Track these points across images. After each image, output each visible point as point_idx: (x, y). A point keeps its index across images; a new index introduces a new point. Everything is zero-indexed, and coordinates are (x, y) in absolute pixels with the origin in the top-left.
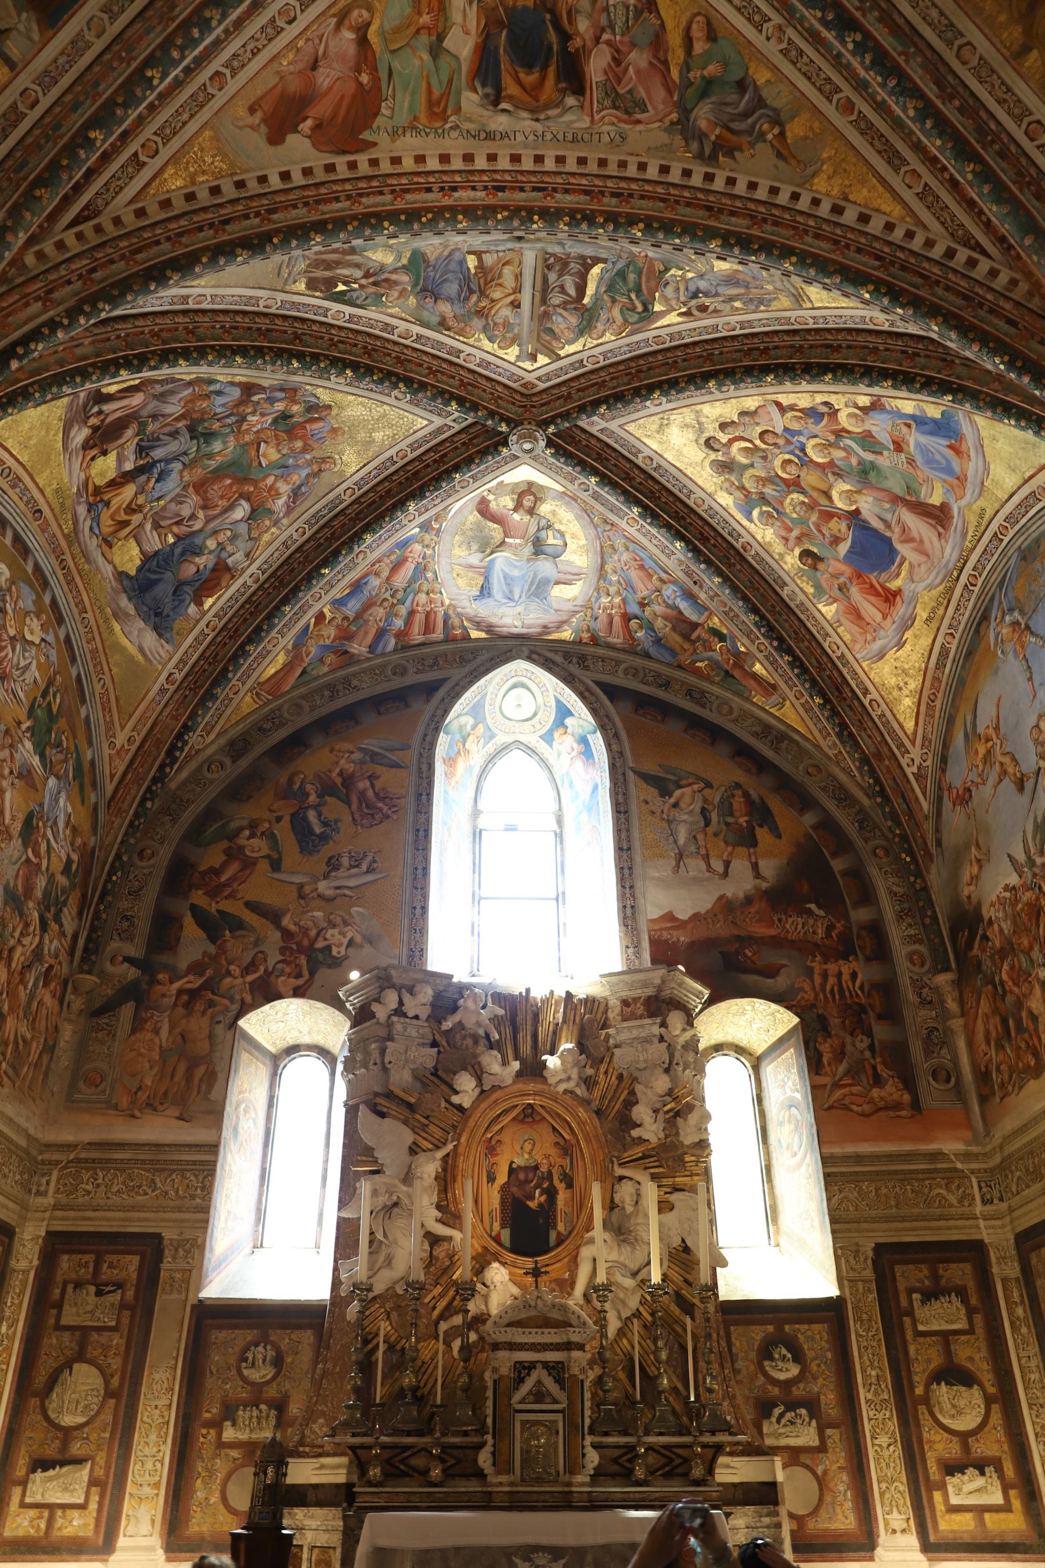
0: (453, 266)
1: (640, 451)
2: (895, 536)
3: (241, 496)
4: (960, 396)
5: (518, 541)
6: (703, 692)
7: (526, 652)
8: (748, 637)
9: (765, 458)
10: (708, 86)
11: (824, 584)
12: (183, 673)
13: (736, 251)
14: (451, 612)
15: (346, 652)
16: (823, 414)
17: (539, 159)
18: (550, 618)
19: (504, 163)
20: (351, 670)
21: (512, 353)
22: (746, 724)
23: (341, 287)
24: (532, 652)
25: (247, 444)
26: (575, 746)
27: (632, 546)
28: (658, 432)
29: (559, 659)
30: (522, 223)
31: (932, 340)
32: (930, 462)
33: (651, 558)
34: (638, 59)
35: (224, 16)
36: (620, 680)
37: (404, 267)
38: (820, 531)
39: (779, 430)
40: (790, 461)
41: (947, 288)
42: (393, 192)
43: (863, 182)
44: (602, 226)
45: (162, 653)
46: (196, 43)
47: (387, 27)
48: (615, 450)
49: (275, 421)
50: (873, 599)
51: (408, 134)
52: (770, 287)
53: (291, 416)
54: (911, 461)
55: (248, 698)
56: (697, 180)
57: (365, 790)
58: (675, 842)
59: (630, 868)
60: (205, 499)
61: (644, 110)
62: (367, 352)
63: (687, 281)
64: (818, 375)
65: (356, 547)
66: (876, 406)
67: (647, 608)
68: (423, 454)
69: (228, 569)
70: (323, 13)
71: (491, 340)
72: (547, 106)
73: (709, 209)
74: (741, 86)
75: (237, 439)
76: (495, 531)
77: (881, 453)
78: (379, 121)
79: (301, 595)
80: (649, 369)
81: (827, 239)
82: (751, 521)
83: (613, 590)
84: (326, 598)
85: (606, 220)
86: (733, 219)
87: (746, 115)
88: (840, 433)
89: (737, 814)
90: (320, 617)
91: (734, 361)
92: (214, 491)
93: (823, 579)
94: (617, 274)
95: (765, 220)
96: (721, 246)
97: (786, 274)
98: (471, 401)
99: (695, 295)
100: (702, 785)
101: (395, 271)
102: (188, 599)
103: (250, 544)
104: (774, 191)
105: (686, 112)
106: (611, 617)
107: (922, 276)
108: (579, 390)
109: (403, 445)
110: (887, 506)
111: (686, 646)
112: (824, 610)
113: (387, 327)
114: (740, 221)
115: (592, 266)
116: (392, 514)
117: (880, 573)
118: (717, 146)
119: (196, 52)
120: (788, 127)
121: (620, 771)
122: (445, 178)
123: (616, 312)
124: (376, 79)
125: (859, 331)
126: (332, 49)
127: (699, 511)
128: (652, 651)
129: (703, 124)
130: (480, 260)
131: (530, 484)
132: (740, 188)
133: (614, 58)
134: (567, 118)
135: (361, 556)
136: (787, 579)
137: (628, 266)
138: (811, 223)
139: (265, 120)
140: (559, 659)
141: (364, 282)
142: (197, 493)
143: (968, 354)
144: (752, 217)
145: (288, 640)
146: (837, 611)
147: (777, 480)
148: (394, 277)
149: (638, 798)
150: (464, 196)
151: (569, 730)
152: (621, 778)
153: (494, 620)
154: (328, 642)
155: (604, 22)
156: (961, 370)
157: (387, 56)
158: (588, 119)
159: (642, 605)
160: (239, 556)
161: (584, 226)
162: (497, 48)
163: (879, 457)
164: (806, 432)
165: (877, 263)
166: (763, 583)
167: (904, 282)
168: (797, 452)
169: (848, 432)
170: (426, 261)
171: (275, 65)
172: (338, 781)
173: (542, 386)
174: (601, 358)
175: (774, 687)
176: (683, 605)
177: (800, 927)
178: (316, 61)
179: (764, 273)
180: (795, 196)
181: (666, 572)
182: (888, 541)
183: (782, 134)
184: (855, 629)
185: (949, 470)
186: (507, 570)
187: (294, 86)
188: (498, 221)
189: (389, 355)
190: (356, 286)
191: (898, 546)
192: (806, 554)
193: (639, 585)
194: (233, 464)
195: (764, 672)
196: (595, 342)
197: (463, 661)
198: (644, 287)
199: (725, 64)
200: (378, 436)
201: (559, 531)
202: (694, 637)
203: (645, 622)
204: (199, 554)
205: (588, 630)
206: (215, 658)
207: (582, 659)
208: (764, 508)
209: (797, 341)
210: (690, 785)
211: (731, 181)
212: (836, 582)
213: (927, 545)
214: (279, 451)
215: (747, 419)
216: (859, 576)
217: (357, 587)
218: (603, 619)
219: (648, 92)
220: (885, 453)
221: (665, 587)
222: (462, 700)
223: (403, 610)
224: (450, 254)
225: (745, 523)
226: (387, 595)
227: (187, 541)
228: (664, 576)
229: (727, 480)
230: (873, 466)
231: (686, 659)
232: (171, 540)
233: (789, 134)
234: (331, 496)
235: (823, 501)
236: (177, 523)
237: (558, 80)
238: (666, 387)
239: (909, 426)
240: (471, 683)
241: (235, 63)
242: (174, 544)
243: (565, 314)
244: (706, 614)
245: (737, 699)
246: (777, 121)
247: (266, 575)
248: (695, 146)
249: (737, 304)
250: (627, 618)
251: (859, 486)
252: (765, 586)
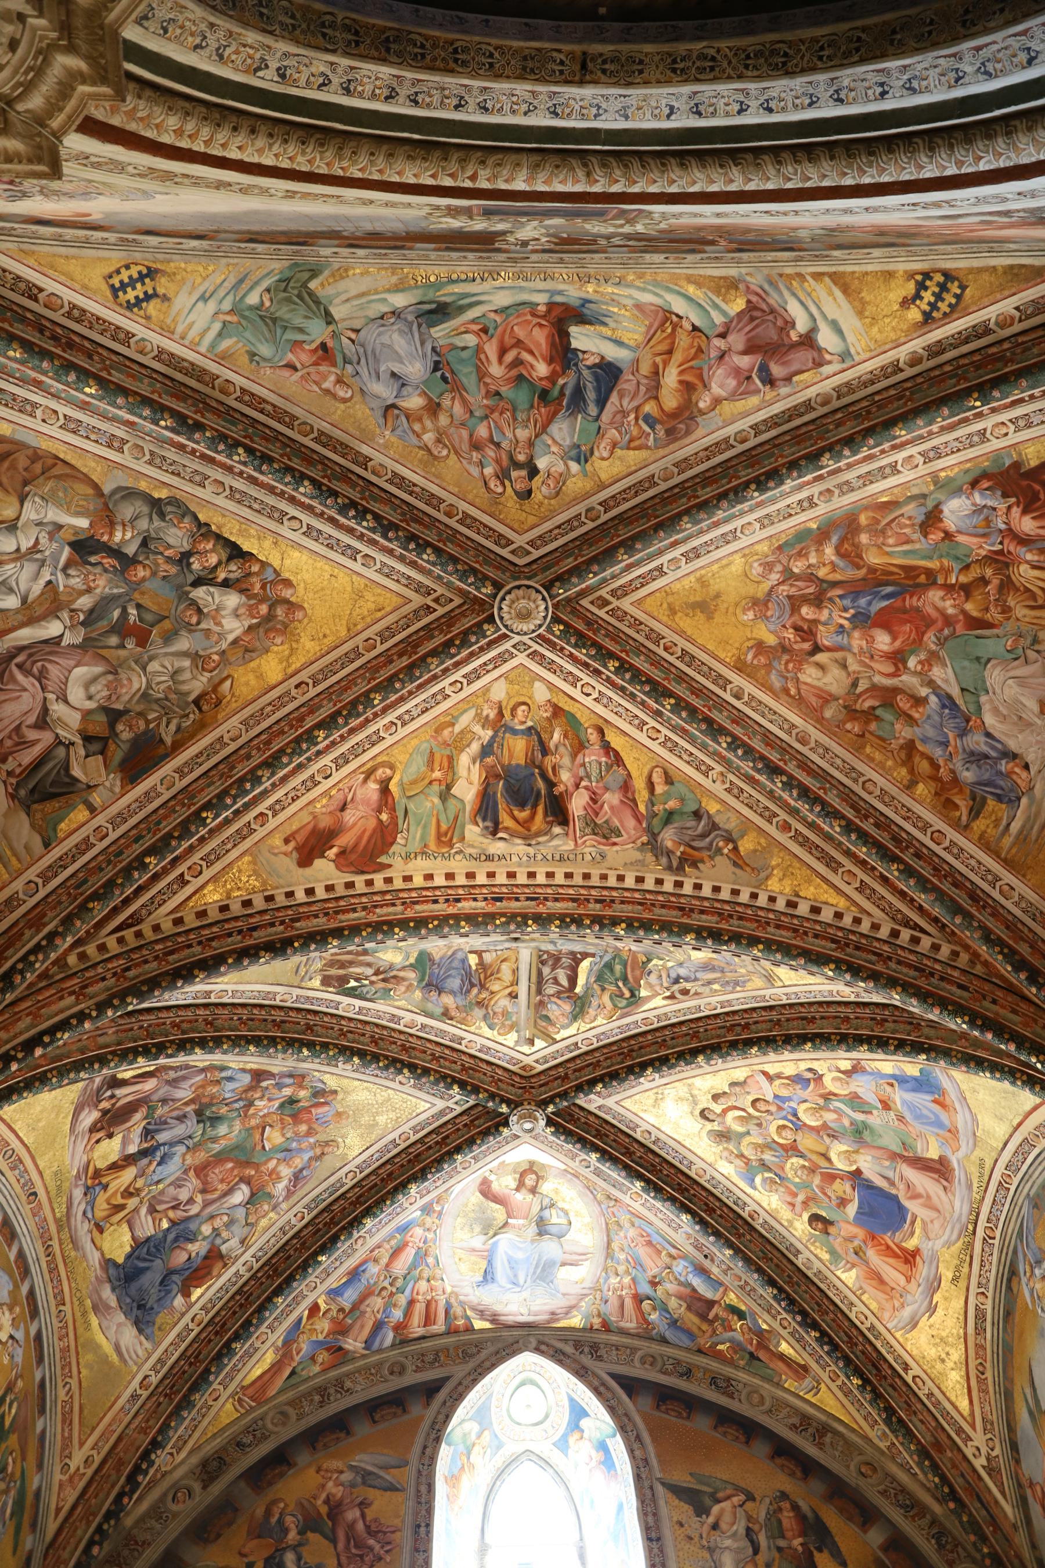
0: (456, 964)
1: (637, 1126)
2: (902, 1195)
3: (242, 1180)
4: (933, 1055)
5: (521, 1222)
6: (728, 1380)
7: (534, 1343)
8: (768, 1312)
9: (760, 1125)
10: (669, 817)
11: (839, 1249)
12: (160, 1376)
13: (709, 942)
14: (453, 1301)
15: (340, 1349)
16: (809, 1080)
17: (532, 875)
18: (557, 1303)
19: (501, 879)
20: (345, 1369)
21: (511, 1038)
22: (781, 1415)
23: (353, 983)
24: (541, 1343)
25: (252, 1128)
26: (593, 1453)
27: (637, 1221)
29: (569, 1349)
30: (518, 926)
31: (896, 1007)
32: (919, 1117)
33: (658, 1233)
34: (612, 798)
35: (273, 774)
36: (637, 1371)
37: (411, 965)
38: (825, 1194)
39: (770, 1097)
40: (784, 1127)
41: (899, 963)
42: (403, 904)
43: (809, 882)
44: (589, 927)
45: (140, 1352)
46: (247, 792)
47: (405, 780)
48: (614, 1126)
49: (282, 1106)
50: (891, 1261)
51: (419, 858)
52: (743, 971)
53: (298, 1101)
54: (901, 1118)
55: (229, 1406)
56: (668, 887)
57: (355, 1521)
60: (205, 1183)
61: (619, 835)
62: (374, 1041)
63: (668, 970)
64: (798, 1044)
65: (355, 1232)
66: (856, 1069)
67: (659, 1287)
68: (425, 1136)
69: (221, 1256)
70: (354, 771)
71: (491, 1027)
72: (538, 834)
73: (681, 909)
74: (697, 815)
75: (243, 1123)
76: (498, 1212)
77: (871, 1113)
78: (395, 848)
79: (295, 1284)
80: (641, 1048)
81: (787, 929)
82: (755, 1188)
83: (621, 1269)
84: (322, 1288)
85: (593, 922)
86: (704, 917)
87: (703, 836)
88: (828, 1096)
90: (314, 1309)
91: (719, 1037)
92: (215, 1174)
93: (837, 1243)
94: (605, 966)
95: (731, 916)
96: (696, 939)
97: (756, 959)
98: (472, 1084)
99: (676, 981)
100: (743, 1497)
101: (403, 969)
102: (175, 1289)
103: (247, 1229)
104: (735, 892)
105: (654, 836)
106: (621, 1299)
107: (875, 954)
108: (575, 1071)
109: (406, 1128)
110: (887, 1163)
111: (705, 1327)
112: (843, 1276)
113: (394, 1018)
114: (709, 918)
115: (582, 960)
116: (393, 1197)
117: (894, 1233)
118: (683, 860)
119: (246, 799)
120: (740, 843)
121: (647, 1484)
122: (450, 892)
123: (606, 998)
124: (394, 818)
125: (829, 1004)
126: (359, 796)
128: (668, 1335)
129: (669, 844)
130: (480, 957)
131: (532, 1163)
132: (706, 891)
133: (591, 799)
134: (555, 842)
135: (360, 1242)
136: (800, 1247)
137: (614, 959)
138: (771, 916)
139: (296, 849)
140: (569, 1349)
141: (374, 978)
142: (198, 1176)
143: (931, 1017)
144: (720, 914)
145: (278, 1336)
146: (857, 1277)
147: (774, 1146)
148: (402, 974)
150: (466, 906)
151: (586, 1435)
152: (648, 1492)
153: (498, 1308)
154: (321, 1337)
155: (582, 772)
156: (926, 1031)
157: (404, 800)
158: (572, 844)
159: (654, 1284)
160: (234, 1243)
161: (573, 928)
162: (495, 793)
164: (795, 1097)
165: (834, 946)
166: (776, 1253)
167: (860, 959)
168: (790, 1117)
169: (835, 1095)
170: (431, 960)
171: (310, 808)
172: (324, 1510)
173: (540, 1068)
175: (805, 1368)
176: (697, 1282)
178: (345, 804)
179: (736, 959)
180: (754, 896)
181: (674, 1247)
182: (895, 1199)
183: (736, 849)
184: (881, 1296)
185: (939, 1124)
186: (510, 1253)
187: (325, 822)
188: (497, 926)
189: (395, 1043)
190: (366, 982)
191: (906, 1203)
192: (815, 1218)
193: (647, 1262)
194: (237, 1147)
195: (791, 1351)
196: (588, 1026)
197: (467, 1356)
198: (629, 976)
199: (682, 800)
200: (382, 1119)
201: (562, 1210)
202: (711, 1316)
203: (658, 1302)
204: (191, 1241)
205: (599, 1315)
206: (197, 1357)
207: (595, 1348)
209: (774, 1015)
210: (728, 1498)
211: (698, 887)
212: (851, 1246)
213: (935, 1199)
214: (283, 1135)
215: (738, 1089)
216: (873, 1238)
217: (354, 1275)
218: (614, 1302)
219: (621, 822)
220: (875, 1112)
221: (675, 1263)
222: (465, 1403)
223: (402, 1300)
224: (454, 954)
225: (749, 1190)
226: (386, 1284)
227: (181, 1227)
228: (673, 1251)
229: (726, 1149)
230: (866, 1126)
231: (705, 1342)
232: (165, 1225)
233: (741, 849)
234: (332, 1180)
235: (823, 1163)
236: (173, 1208)
237: (546, 815)
238: (657, 1064)
239: (892, 1085)
240: (475, 1382)
241: (277, 807)
242: (168, 1229)
243: (559, 1002)
244: (721, 1289)
245: (767, 1386)
246: (729, 839)
247: (260, 1263)
248: (664, 860)
249: (716, 987)
250: (639, 1299)
251: (855, 1147)
252: (779, 1255)
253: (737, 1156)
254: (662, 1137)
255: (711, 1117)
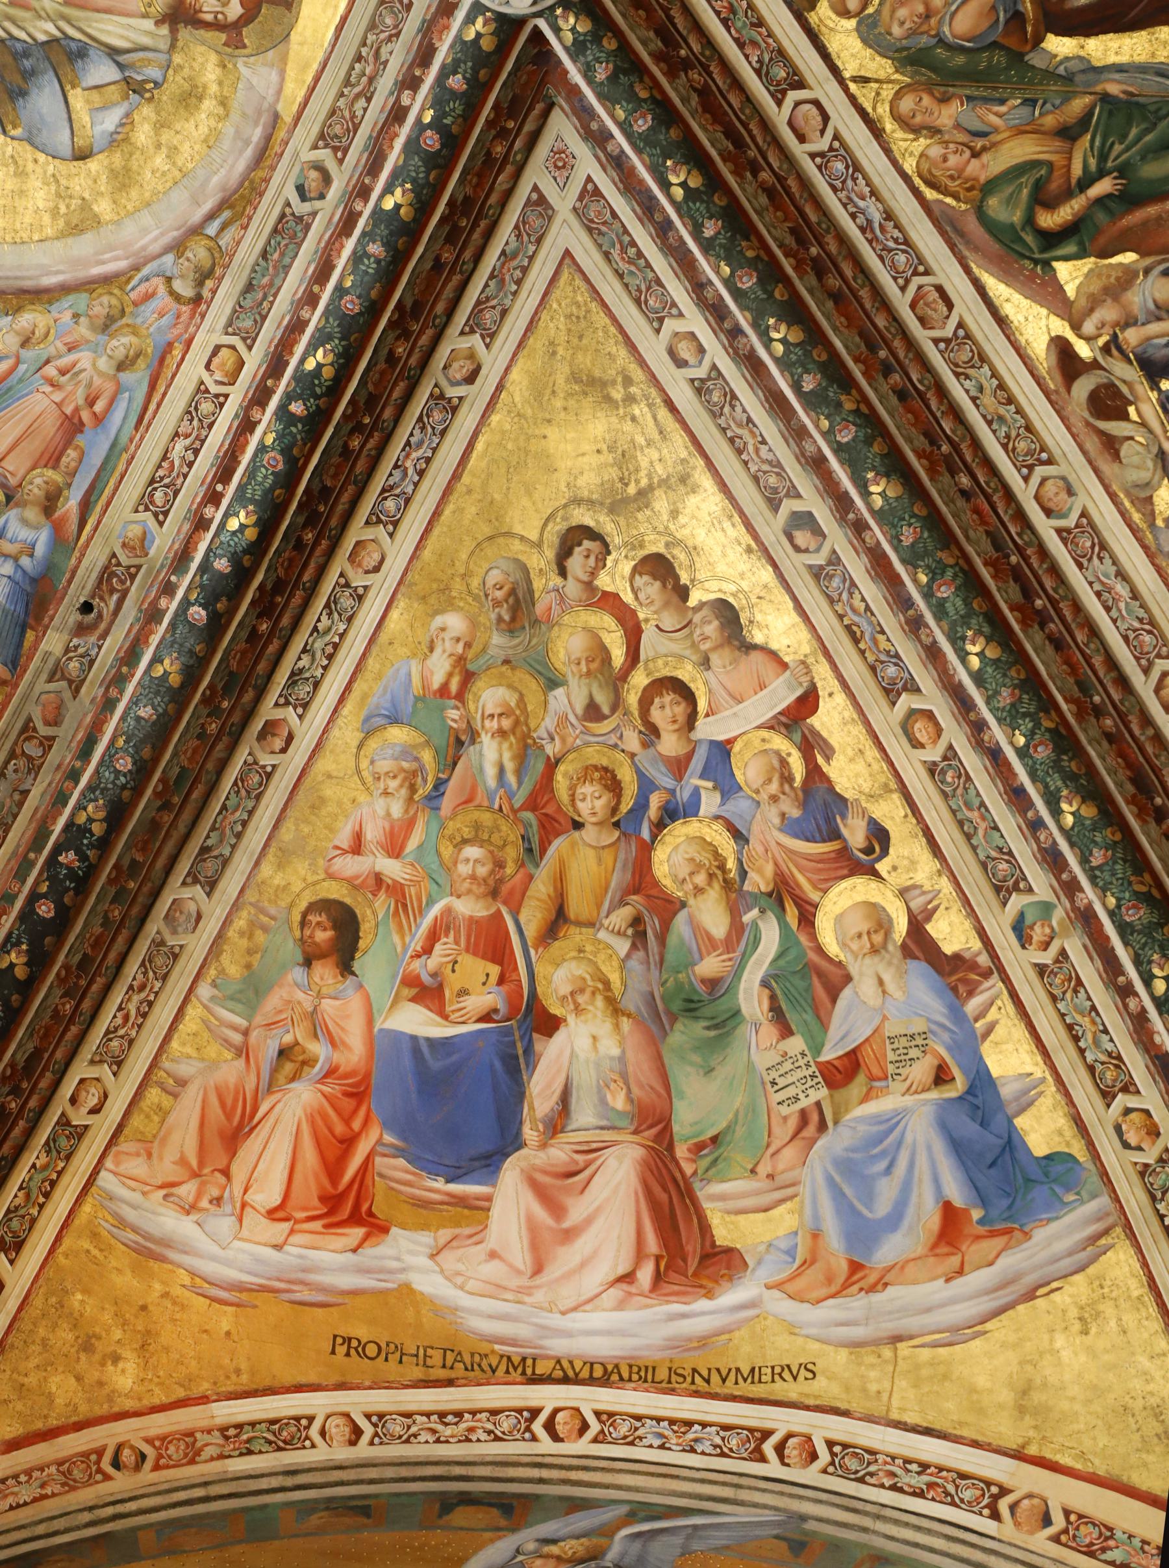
9: (593, 712)
16: (834, 835)
28: (575, 378)
40: (614, 786)
77: (786, 1032)
127: (339, 564)
147: (540, 766)
163: (769, 1032)
169: (807, 919)
174: (823, 144)
181: (86, 506)
196: (883, 110)
208: (427, 757)
215: (712, 629)
220: (796, 1044)
229: (474, 624)
235: (532, 917)
238: (820, 355)
251: (633, 1001)
253: (460, 660)
254: (466, 420)
255: (577, 563)
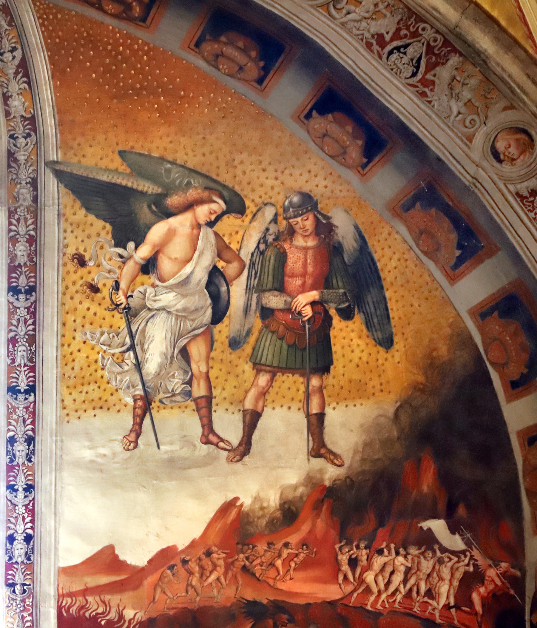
58: (138, 366)
59: (30, 440)
89: (294, 283)
100: (219, 205)
121: (24, 174)
149: (63, 247)
152: (26, 193)
177: (398, 578)
210: (189, 207)
